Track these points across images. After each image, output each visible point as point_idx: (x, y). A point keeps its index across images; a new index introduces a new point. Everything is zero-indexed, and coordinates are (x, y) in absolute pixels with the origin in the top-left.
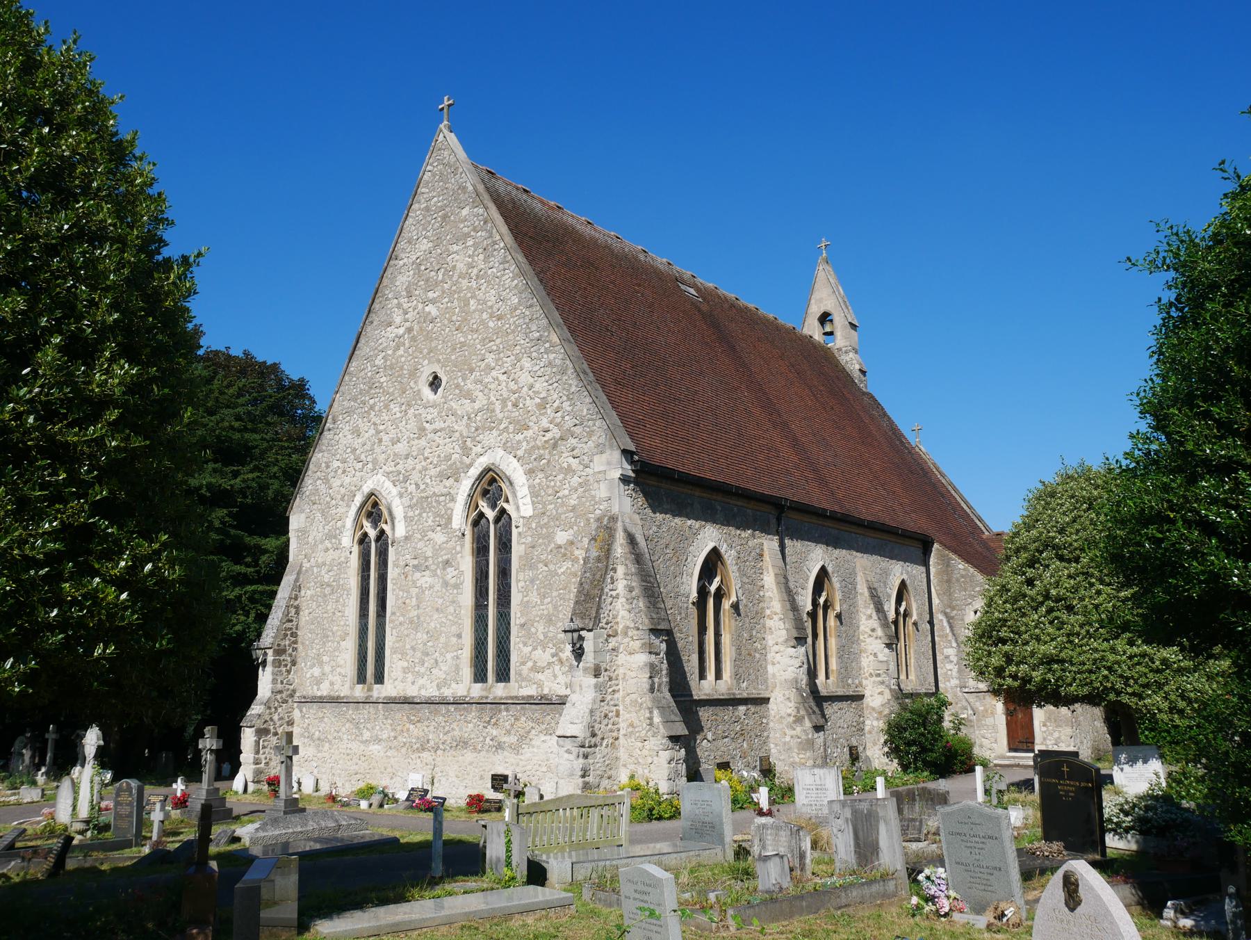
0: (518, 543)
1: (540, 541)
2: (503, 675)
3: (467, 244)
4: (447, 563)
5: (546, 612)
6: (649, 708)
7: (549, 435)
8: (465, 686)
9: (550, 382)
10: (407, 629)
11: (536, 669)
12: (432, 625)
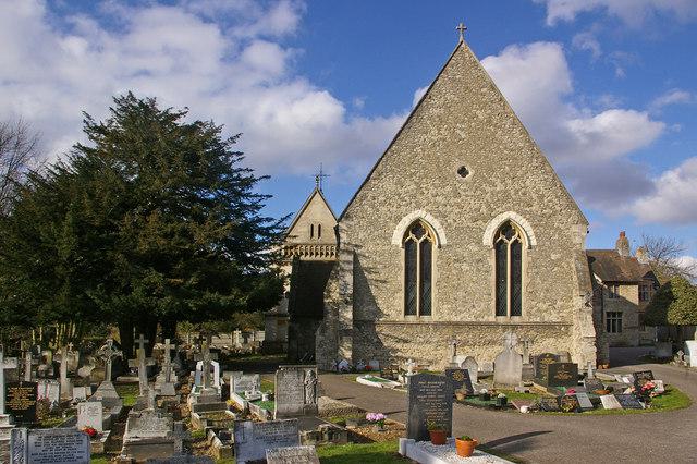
2: (516, 311)
8: (492, 318)
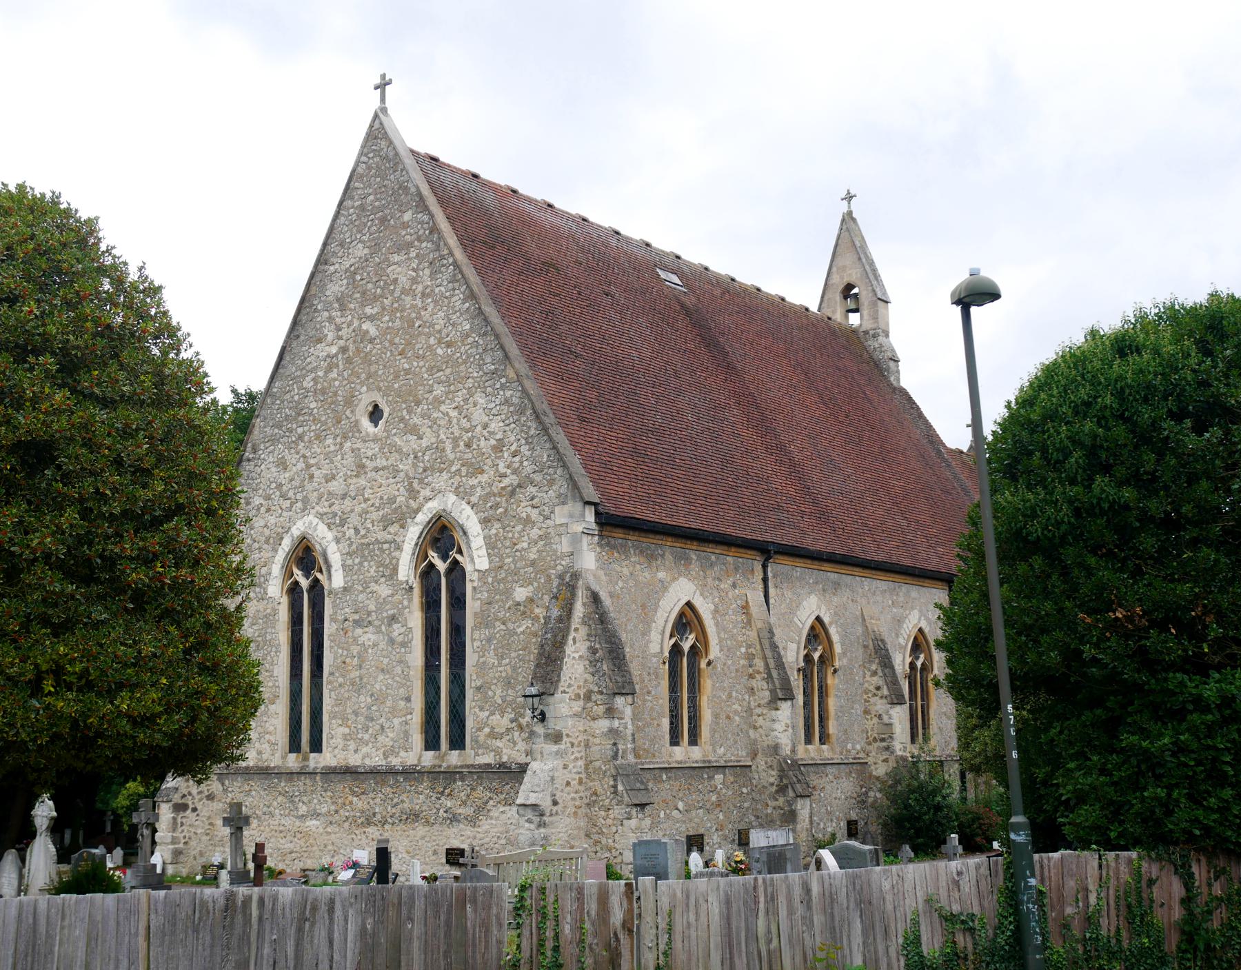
0: (473, 599)
1: (498, 597)
2: (458, 741)
3: (411, 255)
4: (393, 619)
5: (504, 675)
6: (613, 776)
7: (506, 482)
8: (415, 754)
9: (507, 422)
10: (348, 691)
11: (493, 735)
12: (377, 686)
